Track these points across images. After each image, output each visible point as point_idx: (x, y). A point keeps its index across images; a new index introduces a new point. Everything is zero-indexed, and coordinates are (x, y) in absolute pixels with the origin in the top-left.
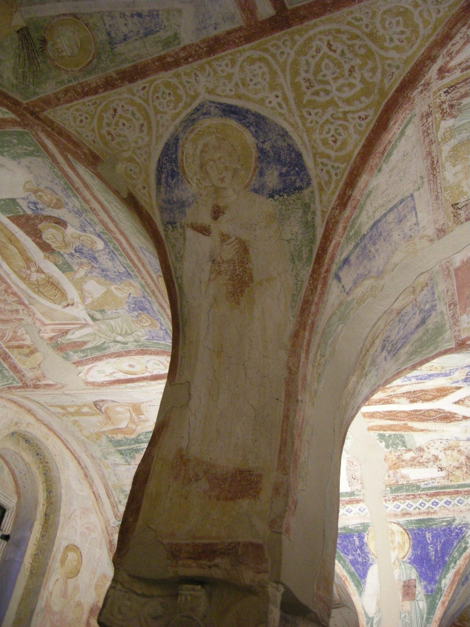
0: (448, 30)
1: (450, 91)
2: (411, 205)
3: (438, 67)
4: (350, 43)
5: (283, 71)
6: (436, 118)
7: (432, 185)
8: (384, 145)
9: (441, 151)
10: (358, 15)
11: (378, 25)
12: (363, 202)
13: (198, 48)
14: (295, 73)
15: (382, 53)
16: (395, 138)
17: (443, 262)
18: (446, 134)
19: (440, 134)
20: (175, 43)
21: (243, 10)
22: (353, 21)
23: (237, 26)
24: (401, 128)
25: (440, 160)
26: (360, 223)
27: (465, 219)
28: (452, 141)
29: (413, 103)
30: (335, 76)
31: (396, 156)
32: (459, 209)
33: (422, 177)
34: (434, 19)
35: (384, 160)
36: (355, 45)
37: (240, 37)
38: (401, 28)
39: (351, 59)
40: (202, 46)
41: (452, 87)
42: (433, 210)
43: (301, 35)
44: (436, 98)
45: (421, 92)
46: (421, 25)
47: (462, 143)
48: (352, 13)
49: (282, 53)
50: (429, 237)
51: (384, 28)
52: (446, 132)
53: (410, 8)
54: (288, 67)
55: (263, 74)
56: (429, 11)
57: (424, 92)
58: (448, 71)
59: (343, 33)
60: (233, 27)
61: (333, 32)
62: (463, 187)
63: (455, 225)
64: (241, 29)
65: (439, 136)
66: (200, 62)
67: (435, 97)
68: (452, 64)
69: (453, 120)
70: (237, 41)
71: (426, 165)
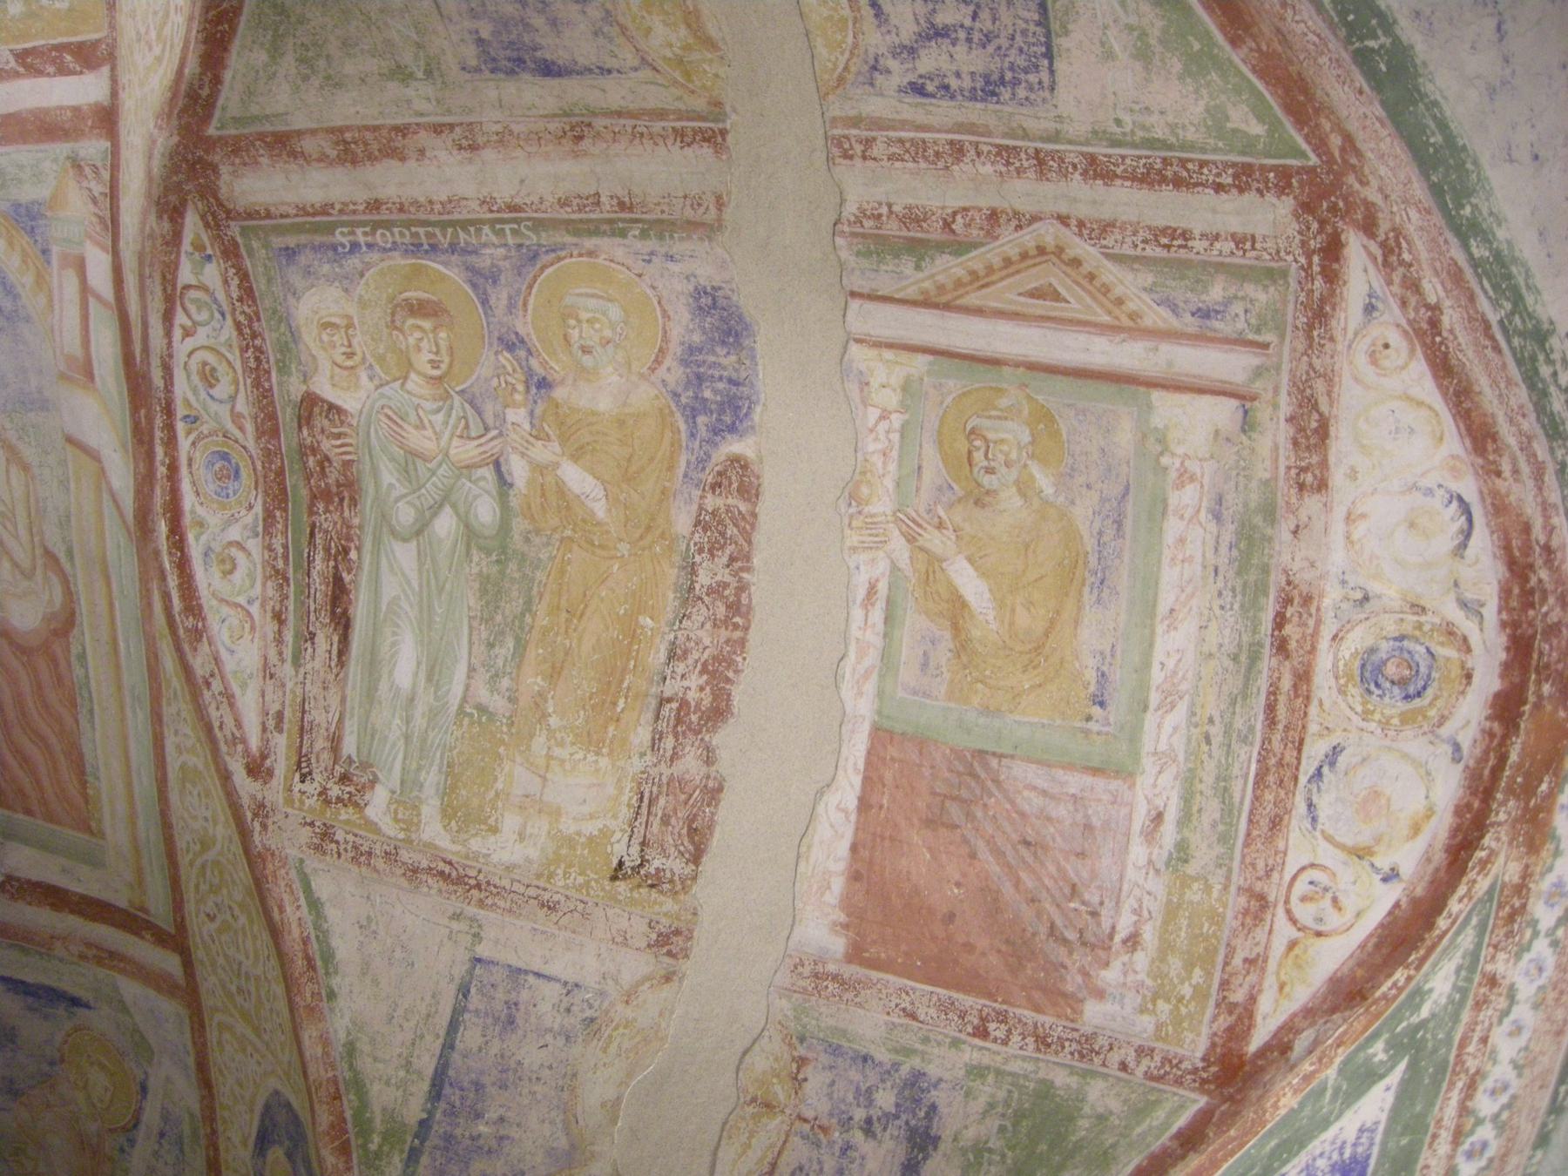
1: (305, 770)
2: (498, 975)
3: (243, 773)
6: (348, 822)
7: (501, 903)
8: (300, 955)
9: (430, 845)
12: (348, 1075)
16: (310, 925)
17: (784, 979)
18: (400, 816)
19: (389, 828)
24: (303, 901)
25: (450, 857)
26: (384, 1109)
27: (688, 861)
28: (426, 810)
29: (273, 855)
31: (344, 947)
32: (641, 865)
33: (456, 917)
35: (327, 974)
41: (299, 763)
42: (574, 932)
44: (302, 803)
45: (264, 827)
47: (448, 791)
50: (648, 978)
52: (396, 812)
57: (270, 822)
58: (264, 757)
62: (579, 834)
63: (682, 897)
65: (392, 833)
67: (297, 804)
68: (254, 743)
69: (378, 787)
71: (433, 892)
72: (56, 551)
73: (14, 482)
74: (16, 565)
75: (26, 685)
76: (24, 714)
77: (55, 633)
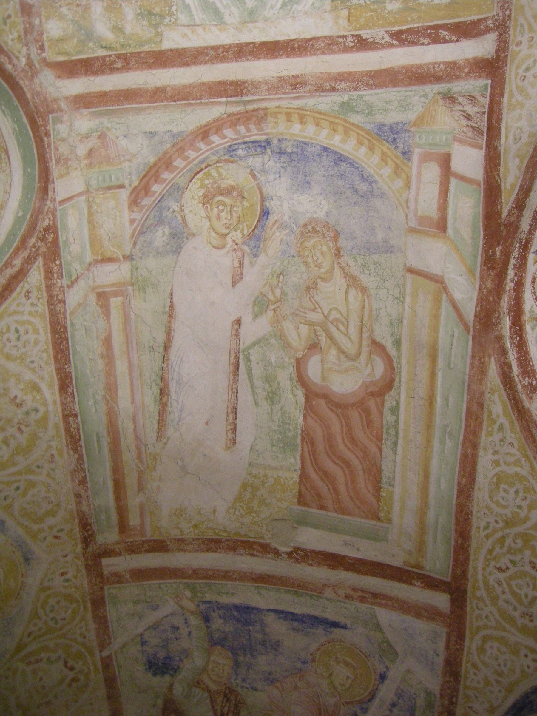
0: (535, 444)
4: (505, 549)
5: (505, 630)
10: (483, 524)
11: (500, 510)
13: (447, 685)
14: (512, 620)
15: (529, 524)
20: (433, 698)
21: (433, 619)
22: (487, 532)
23: (444, 635)
30: (531, 585)
34: (518, 453)
36: (510, 544)
37: (456, 641)
38: (512, 491)
39: (523, 558)
40: (447, 679)
43: (478, 589)
46: (518, 469)
48: (478, 528)
49: (487, 617)
51: (506, 507)
53: (497, 469)
54: (502, 621)
55: (499, 649)
56: (507, 454)
59: (493, 548)
60: (444, 640)
61: (489, 557)
64: (449, 635)
66: (461, 693)
70: (458, 647)
72: (383, 342)
73: (351, 298)
74: (341, 351)
75: (336, 428)
76: (331, 446)
77: (372, 394)
